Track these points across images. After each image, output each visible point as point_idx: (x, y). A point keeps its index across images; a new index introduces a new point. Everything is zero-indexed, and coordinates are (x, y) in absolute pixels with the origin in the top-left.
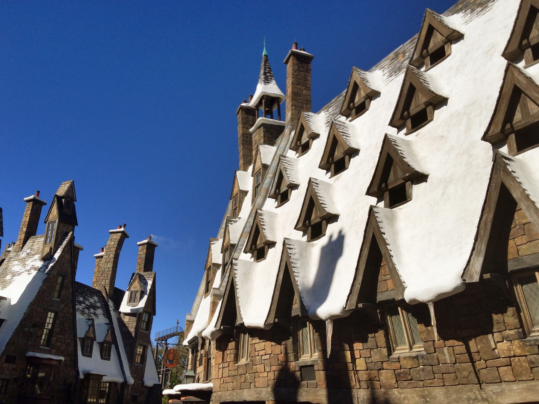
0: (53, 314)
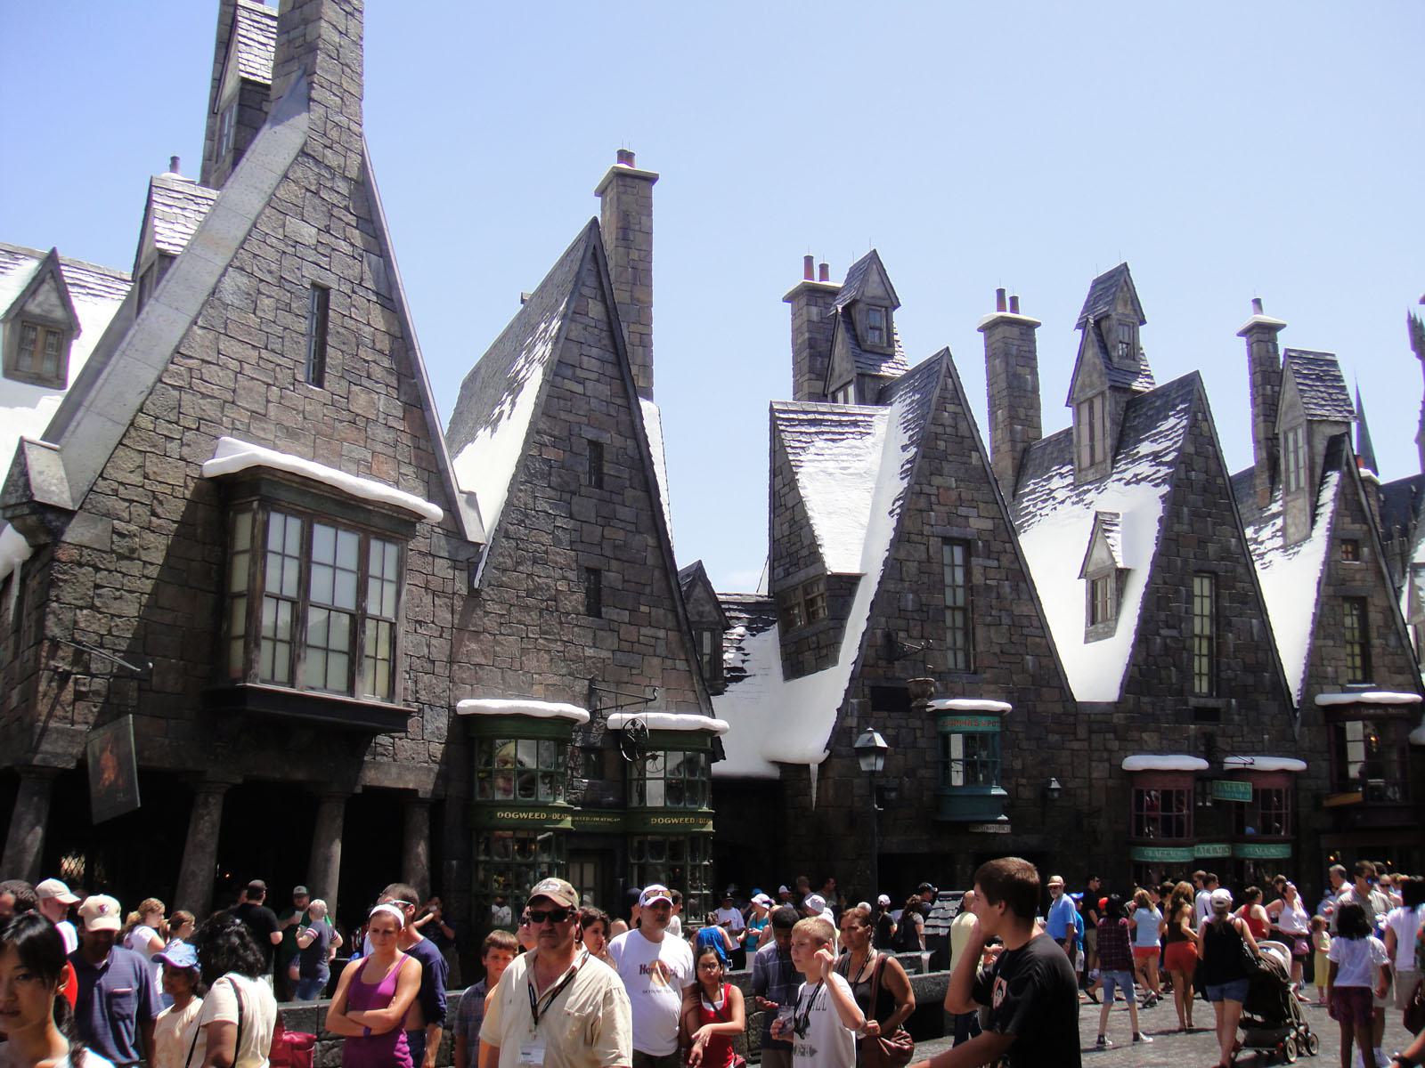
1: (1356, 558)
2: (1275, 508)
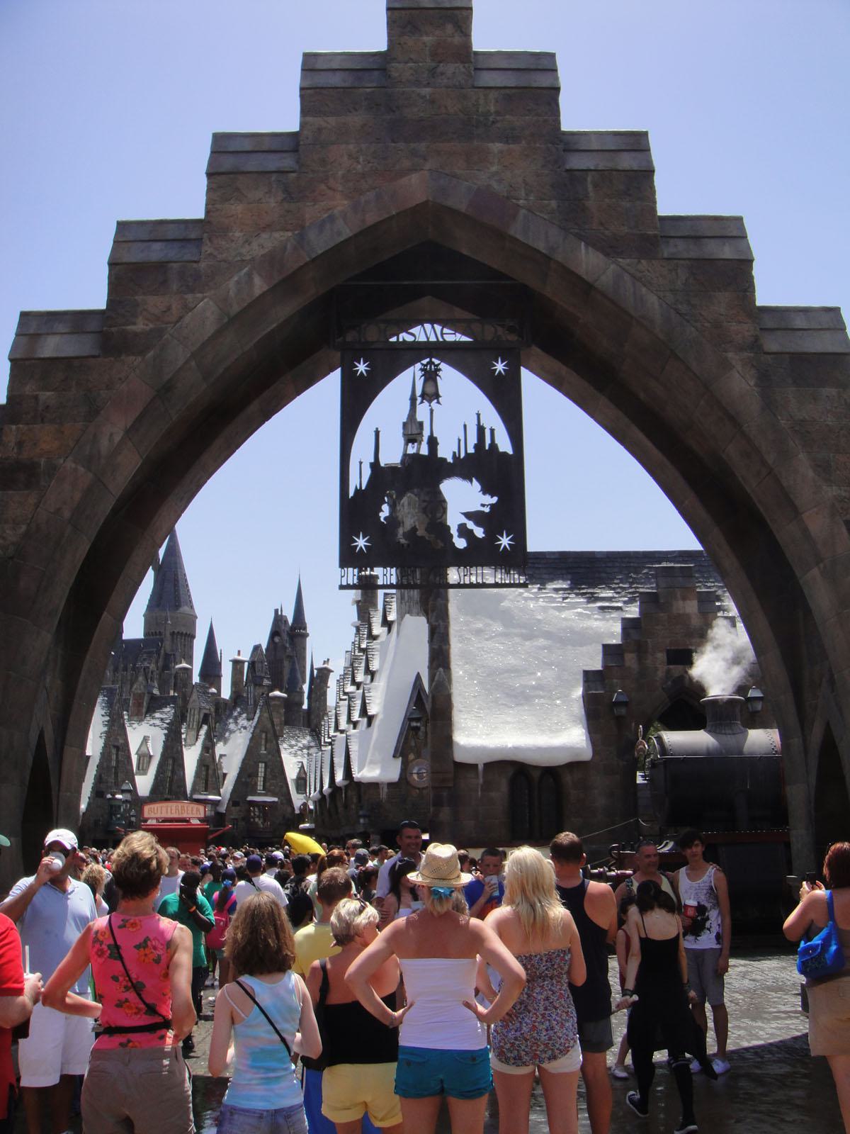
0: (263, 764)
1: (208, 753)
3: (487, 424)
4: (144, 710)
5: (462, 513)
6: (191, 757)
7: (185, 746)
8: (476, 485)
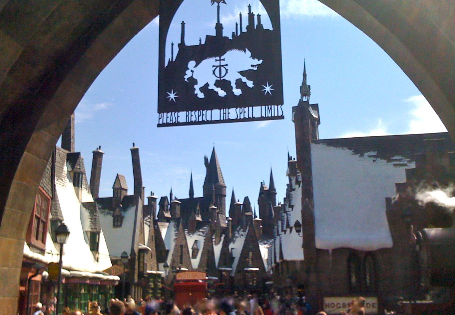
2: (213, 237)
3: (255, 12)
4: (195, 228)
5: (239, 72)
6: (217, 249)
7: (215, 244)
8: (248, 53)
